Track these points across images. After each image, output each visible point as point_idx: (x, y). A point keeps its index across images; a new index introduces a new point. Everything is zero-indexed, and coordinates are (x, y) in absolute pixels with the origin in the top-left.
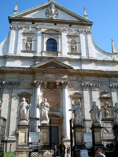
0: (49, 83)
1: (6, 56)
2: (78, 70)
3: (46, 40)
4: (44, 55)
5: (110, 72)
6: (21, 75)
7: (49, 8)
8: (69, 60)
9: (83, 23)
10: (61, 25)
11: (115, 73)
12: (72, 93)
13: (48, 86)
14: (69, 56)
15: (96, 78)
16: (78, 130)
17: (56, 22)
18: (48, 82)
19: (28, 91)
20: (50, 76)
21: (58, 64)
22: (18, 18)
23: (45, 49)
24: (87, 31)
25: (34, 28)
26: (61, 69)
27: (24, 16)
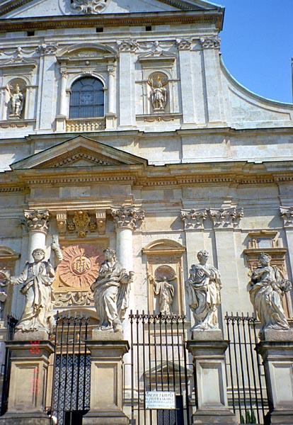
0: (73, 216)
3: (67, 83)
4: (61, 128)
5: (277, 167)
9: (192, 17)
12: (146, 242)
14: (143, 127)
18: (68, 212)
20: (76, 191)
21: (98, 151)
23: (65, 111)
26: (109, 169)
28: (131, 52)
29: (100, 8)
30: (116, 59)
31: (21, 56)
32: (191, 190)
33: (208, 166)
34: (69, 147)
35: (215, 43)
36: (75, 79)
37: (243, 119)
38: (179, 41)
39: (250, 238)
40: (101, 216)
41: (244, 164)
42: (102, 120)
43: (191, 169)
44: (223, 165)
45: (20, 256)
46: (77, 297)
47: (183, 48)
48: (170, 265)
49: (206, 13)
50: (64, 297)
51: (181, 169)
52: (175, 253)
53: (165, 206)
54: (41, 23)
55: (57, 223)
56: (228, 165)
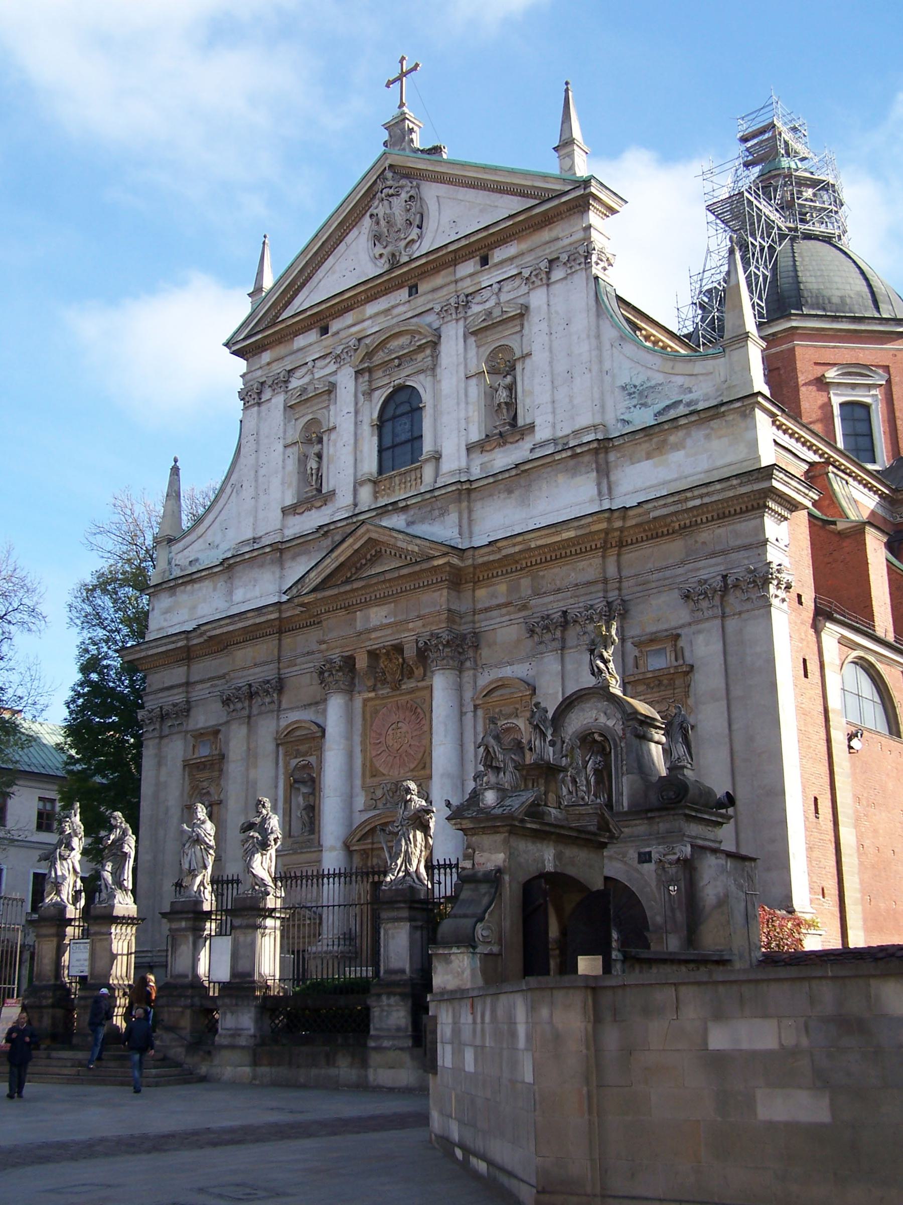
3: (372, 411)
5: (665, 505)
10: (439, 280)
11: (697, 502)
13: (377, 676)
15: (611, 561)
19: (313, 719)
20: (378, 615)
21: (392, 541)
22: (260, 336)
23: (370, 464)
25: (328, 360)
28: (457, 320)
29: (413, 241)
30: (435, 344)
31: (317, 376)
33: (553, 530)
36: (383, 399)
37: (635, 406)
38: (526, 273)
40: (410, 652)
41: (606, 515)
43: (530, 540)
44: (576, 524)
45: (323, 731)
47: (536, 285)
49: (564, 199)
50: (379, 793)
51: (514, 545)
53: (509, 613)
56: (583, 522)
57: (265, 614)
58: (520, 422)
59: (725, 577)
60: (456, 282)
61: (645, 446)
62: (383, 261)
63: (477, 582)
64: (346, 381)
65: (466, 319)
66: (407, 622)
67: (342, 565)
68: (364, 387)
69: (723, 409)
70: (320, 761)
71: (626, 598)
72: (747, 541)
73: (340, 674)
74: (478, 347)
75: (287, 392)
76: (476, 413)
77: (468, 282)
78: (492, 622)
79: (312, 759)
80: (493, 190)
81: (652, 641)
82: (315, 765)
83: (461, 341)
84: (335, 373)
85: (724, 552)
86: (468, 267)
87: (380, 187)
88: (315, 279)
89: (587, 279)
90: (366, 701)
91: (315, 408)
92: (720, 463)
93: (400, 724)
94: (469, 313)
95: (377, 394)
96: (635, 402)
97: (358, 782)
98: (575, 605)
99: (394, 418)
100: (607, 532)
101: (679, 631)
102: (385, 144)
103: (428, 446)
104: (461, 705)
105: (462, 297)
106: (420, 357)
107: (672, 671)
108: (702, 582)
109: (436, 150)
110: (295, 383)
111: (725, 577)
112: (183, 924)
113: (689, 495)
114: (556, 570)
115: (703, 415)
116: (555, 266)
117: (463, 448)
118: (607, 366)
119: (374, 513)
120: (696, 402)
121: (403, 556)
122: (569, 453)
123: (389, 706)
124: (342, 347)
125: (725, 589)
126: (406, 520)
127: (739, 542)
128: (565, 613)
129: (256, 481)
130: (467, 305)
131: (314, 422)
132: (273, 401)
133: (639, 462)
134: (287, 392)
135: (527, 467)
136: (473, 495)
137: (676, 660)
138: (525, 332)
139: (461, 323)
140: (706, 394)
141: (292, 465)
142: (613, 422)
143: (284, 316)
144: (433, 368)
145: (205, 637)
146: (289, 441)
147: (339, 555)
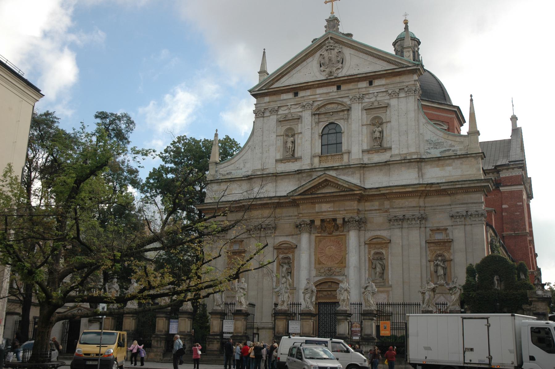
1: (251, 177)
2: (377, 188)
5: (448, 185)
6: (278, 211)
7: (323, 51)
8: (363, 167)
10: (351, 86)
11: (460, 186)
14: (366, 159)
15: (422, 200)
16: (279, 317)
17: (339, 84)
20: (325, 207)
21: (336, 182)
22: (266, 91)
23: (318, 150)
24: (406, 89)
25: (297, 106)
27: (277, 81)
31: (292, 111)
32: (395, 202)
34: (319, 180)
35: (415, 91)
38: (390, 92)
39: (431, 233)
40: (340, 222)
41: (425, 185)
42: (341, 154)
44: (413, 187)
45: (297, 246)
46: (328, 270)
48: (381, 250)
49: (408, 69)
50: (322, 271)
51: (387, 190)
52: (385, 243)
53: (379, 213)
54: (302, 86)
55: (316, 227)
57: (272, 200)
58: (385, 145)
59: (467, 212)
60: (359, 89)
61: (437, 162)
62: (324, 73)
63: (366, 201)
64: (307, 115)
65: (362, 103)
66: (340, 211)
67: (312, 187)
68: (317, 120)
69: (468, 156)
70: (293, 256)
71: (427, 213)
72: (475, 201)
73: (308, 226)
74: (367, 115)
75: (277, 115)
76: (366, 139)
77: (364, 90)
78: (372, 215)
79: (290, 256)
80: (375, 57)
81: (438, 230)
82: (291, 258)
83: (360, 111)
84: (302, 112)
85: (466, 203)
86: (364, 84)
87: (327, 45)
88: (292, 73)
89: (415, 99)
90: (317, 237)
91: (291, 124)
92: (465, 173)
93: (332, 247)
94: (363, 102)
95: (321, 123)
96: (432, 146)
97: (313, 266)
98: (409, 214)
99: (328, 134)
100: (423, 191)
101: (447, 227)
102: (326, 27)
103: (344, 148)
104: (359, 243)
105: (361, 95)
106: (341, 114)
107: (446, 240)
108: (458, 213)
109: (350, 35)
110: (281, 112)
111: (467, 212)
112: (342, 317)
113: (457, 183)
114: (400, 200)
115: (461, 156)
116: (401, 91)
117: (361, 151)
118: (421, 132)
119: (323, 169)
120: (457, 151)
121: (339, 187)
122: (407, 161)
123: (327, 239)
124: (305, 103)
125: (467, 215)
126: (336, 173)
127: (472, 201)
128: (404, 215)
129: (262, 147)
130: (363, 98)
131: (290, 129)
132: (271, 117)
133: (434, 167)
134: (277, 115)
135: (390, 163)
136: (365, 169)
137: (447, 236)
138: (388, 113)
139: (360, 104)
140: (461, 150)
141: (280, 143)
142: (423, 151)
143: (276, 85)
144: (348, 119)
145: (241, 204)
146: (279, 134)
147: (312, 183)
